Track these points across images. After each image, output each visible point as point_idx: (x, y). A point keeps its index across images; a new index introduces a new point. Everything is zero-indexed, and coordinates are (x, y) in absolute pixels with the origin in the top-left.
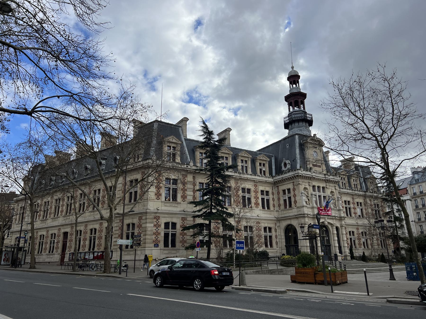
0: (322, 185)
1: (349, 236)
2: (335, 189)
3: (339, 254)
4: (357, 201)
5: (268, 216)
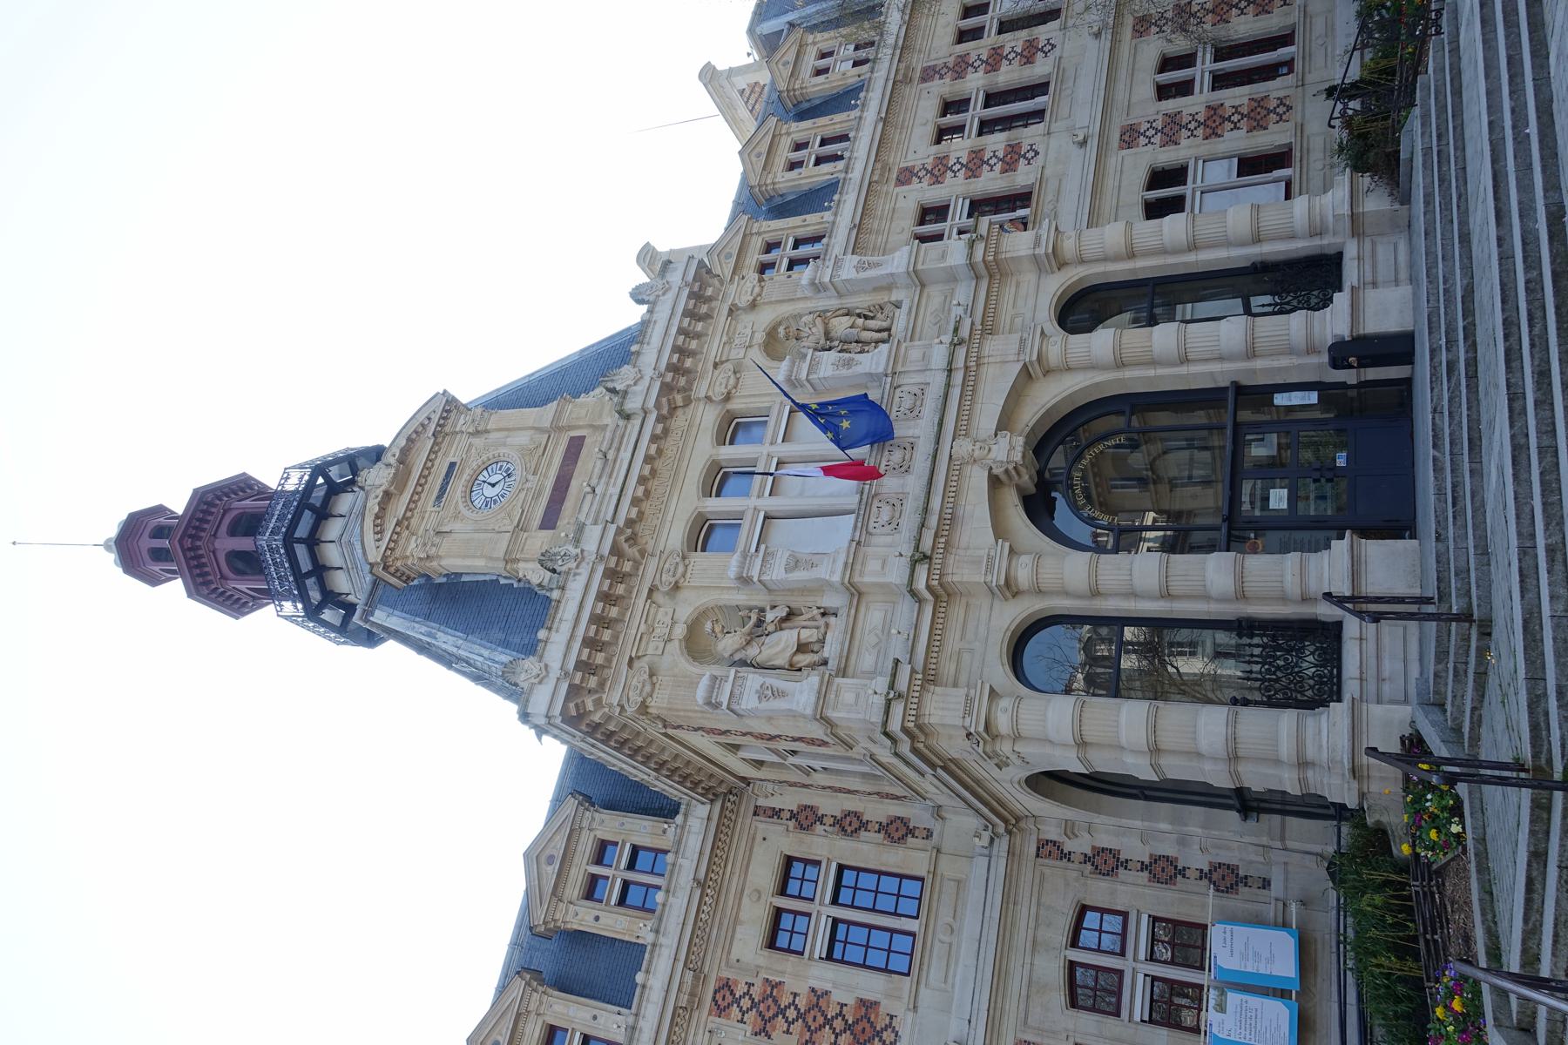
0: (700, 447)
1: (1192, 105)
2: (753, 305)
3: (1334, 321)
4: (950, 36)
5: (970, 923)
